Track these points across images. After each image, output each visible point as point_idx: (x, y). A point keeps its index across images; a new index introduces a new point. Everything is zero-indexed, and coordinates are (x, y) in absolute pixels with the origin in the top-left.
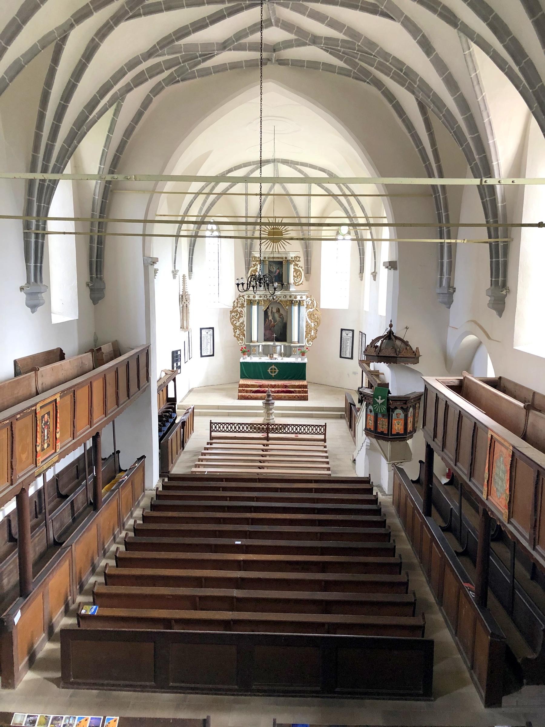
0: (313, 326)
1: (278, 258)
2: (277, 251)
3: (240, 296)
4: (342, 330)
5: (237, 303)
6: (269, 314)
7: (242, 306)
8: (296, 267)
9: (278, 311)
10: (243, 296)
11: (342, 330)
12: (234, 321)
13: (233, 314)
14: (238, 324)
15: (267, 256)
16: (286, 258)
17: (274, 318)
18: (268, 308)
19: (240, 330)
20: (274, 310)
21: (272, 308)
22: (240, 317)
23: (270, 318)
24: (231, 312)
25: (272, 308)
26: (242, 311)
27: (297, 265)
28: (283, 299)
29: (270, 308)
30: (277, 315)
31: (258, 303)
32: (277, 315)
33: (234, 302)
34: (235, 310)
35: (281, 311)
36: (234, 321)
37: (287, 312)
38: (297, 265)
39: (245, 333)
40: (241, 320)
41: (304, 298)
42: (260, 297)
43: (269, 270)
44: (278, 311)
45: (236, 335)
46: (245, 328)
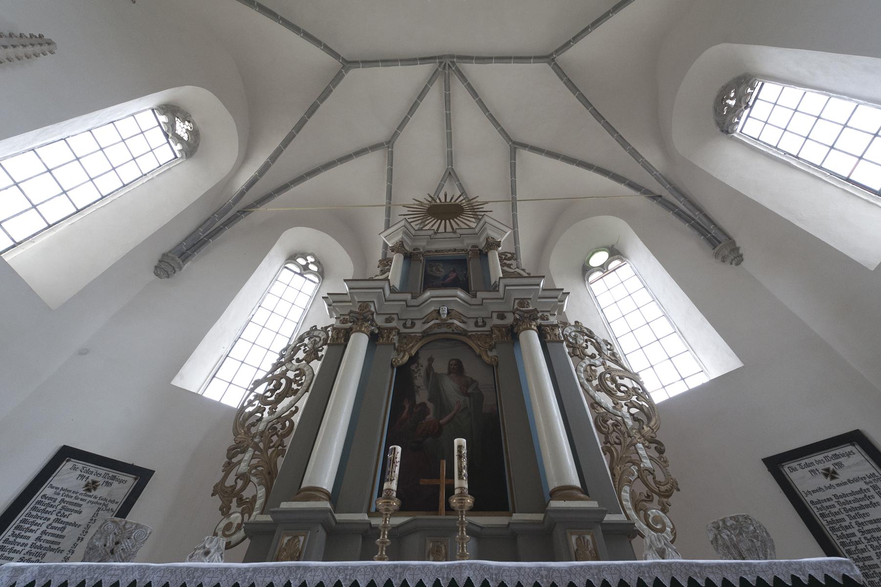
0: (630, 422)
1: (455, 250)
2: (449, 229)
4: (775, 464)
6: (419, 381)
7: (312, 355)
8: (506, 268)
9: (457, 369)
11: (775, 464)
15: (422, 244)
16: (474, 246)
17: (437, 395)
18: (413, 359)
20: (441, 367)
21: (431, 360)
23: (422, 397)
25: (431, 360)
27: (509, 266)
28: (471, 327)
29: (423, 361)
30: (450, 386)
31: (374, 339)
32: (450, 386)
35: (472, 370)
37: (493, 367)
38: (509, 266)
41: (553, 320)
42: (388, 320)
43: (426, 272)
44: (457, 369)
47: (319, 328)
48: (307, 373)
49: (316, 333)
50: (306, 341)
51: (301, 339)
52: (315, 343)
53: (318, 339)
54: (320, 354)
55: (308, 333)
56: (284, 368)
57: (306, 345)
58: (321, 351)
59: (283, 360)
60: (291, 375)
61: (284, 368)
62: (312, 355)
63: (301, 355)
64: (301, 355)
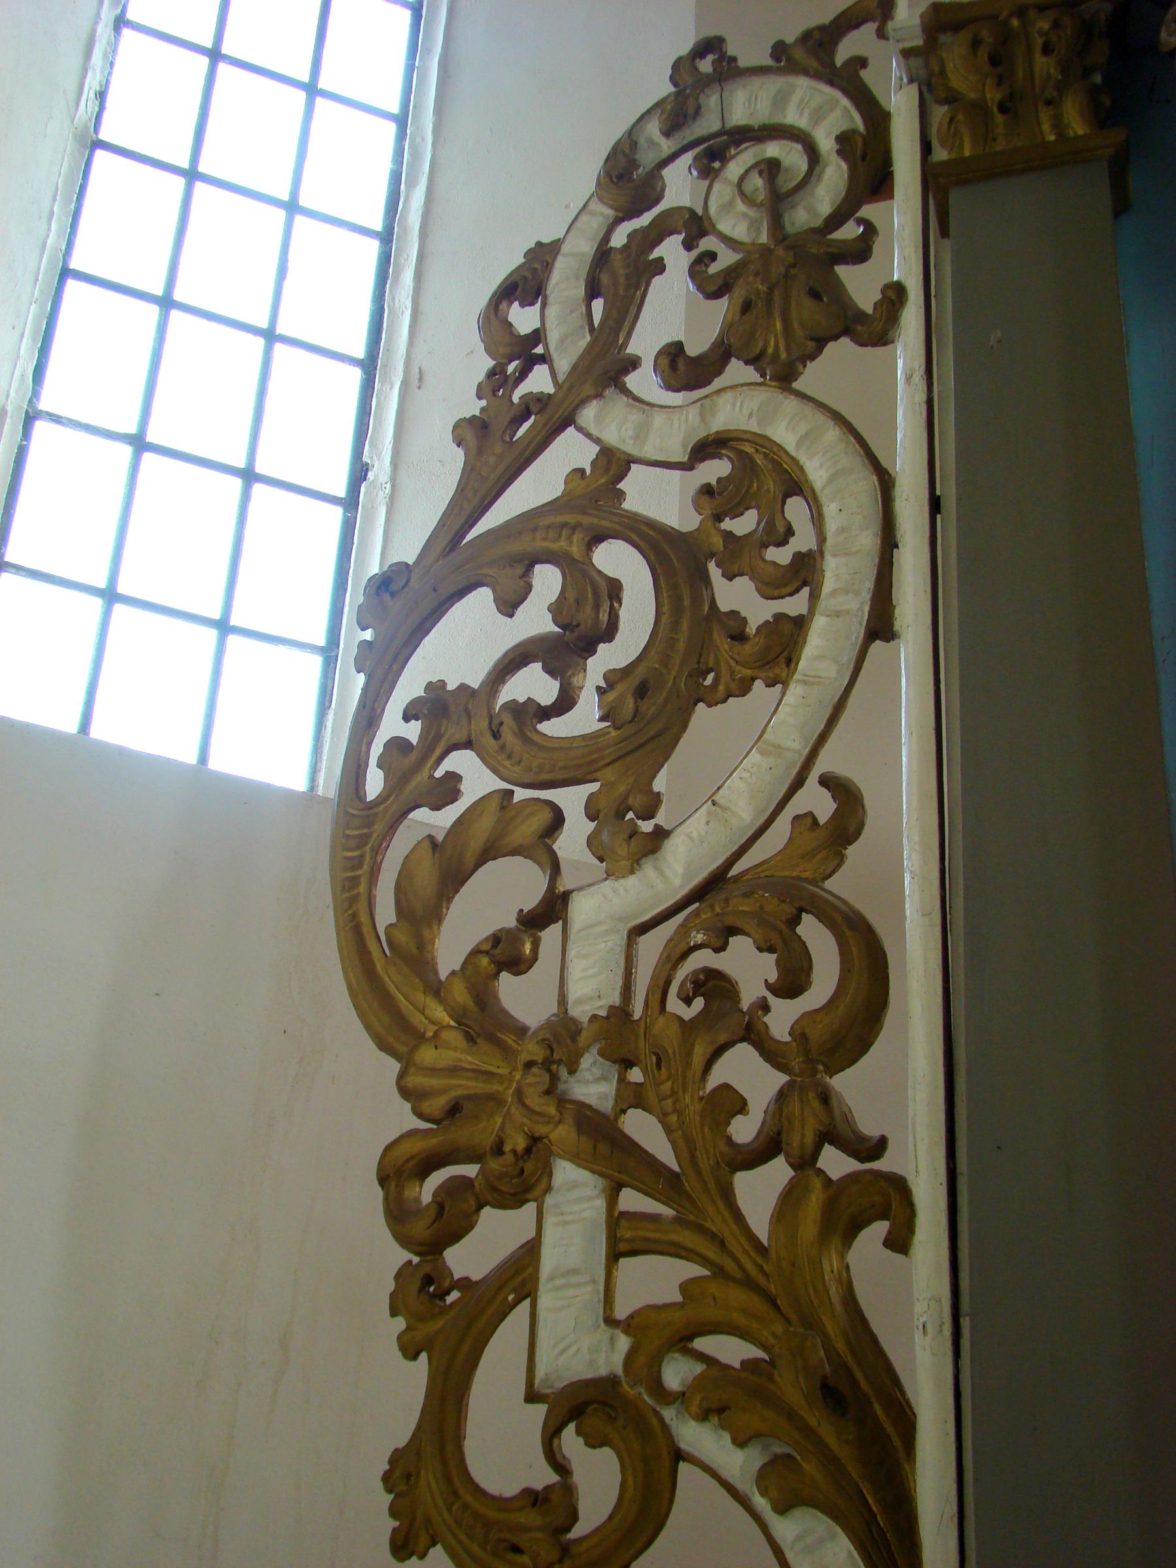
3: (708, 65)
5: (620, 279)
7: (792, 303)
10: (814, 53)
12: (453, 864)
13: (467, 642)
14: (584, 971)
19: (678, 1202)
22: (704, 661)
24: (401, 607)
26: (753, 476)
33: (526, 285)
34: (539, 485)
36: (453, 864)
39: (907, 1297)
40: (727, 781)
45: (503, 1449)
46: (900, 1091)
47: (749, 51)
48: (816, 472)
49: (745, 104)
50: (680, 186)
51: (627, 180)
52: (778, 199)
53: (792, 156)
54: (861, 286)
55: (677, 113)
56: (570, 453)
57: (695, 226)
58: (860, 252)
59: (539, 381)
60: (660, 497)
61: (570, 453)
62: (792, 303)
63: (673, 311)
64: (673, 311)
